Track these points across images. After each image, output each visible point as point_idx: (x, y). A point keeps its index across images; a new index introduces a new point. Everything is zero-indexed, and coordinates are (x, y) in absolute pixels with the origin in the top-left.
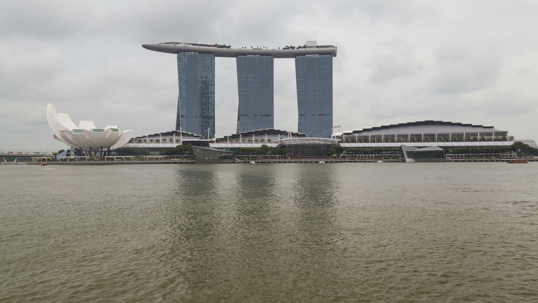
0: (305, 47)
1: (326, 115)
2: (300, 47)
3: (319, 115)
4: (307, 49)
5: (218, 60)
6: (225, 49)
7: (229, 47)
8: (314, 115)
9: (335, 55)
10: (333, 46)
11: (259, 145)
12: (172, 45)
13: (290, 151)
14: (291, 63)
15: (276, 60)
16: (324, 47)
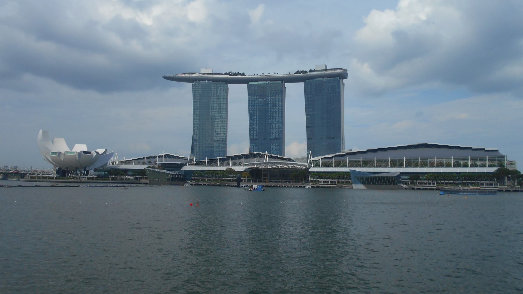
0: (314, 71)
1: (334, 138)
2: (310, 71)
3: (327, 138)
4: (315, 73)
5: (232, 87)
6: (239, 76)
7: (243, 74)
8: (321, 139)
9: (346, 78)
10: (340, 69)
11: (224, 168)
12: (188, 75)
13: (265, 175)
14: (300, 87)
15: (287, 85)
16: (331, 70)
